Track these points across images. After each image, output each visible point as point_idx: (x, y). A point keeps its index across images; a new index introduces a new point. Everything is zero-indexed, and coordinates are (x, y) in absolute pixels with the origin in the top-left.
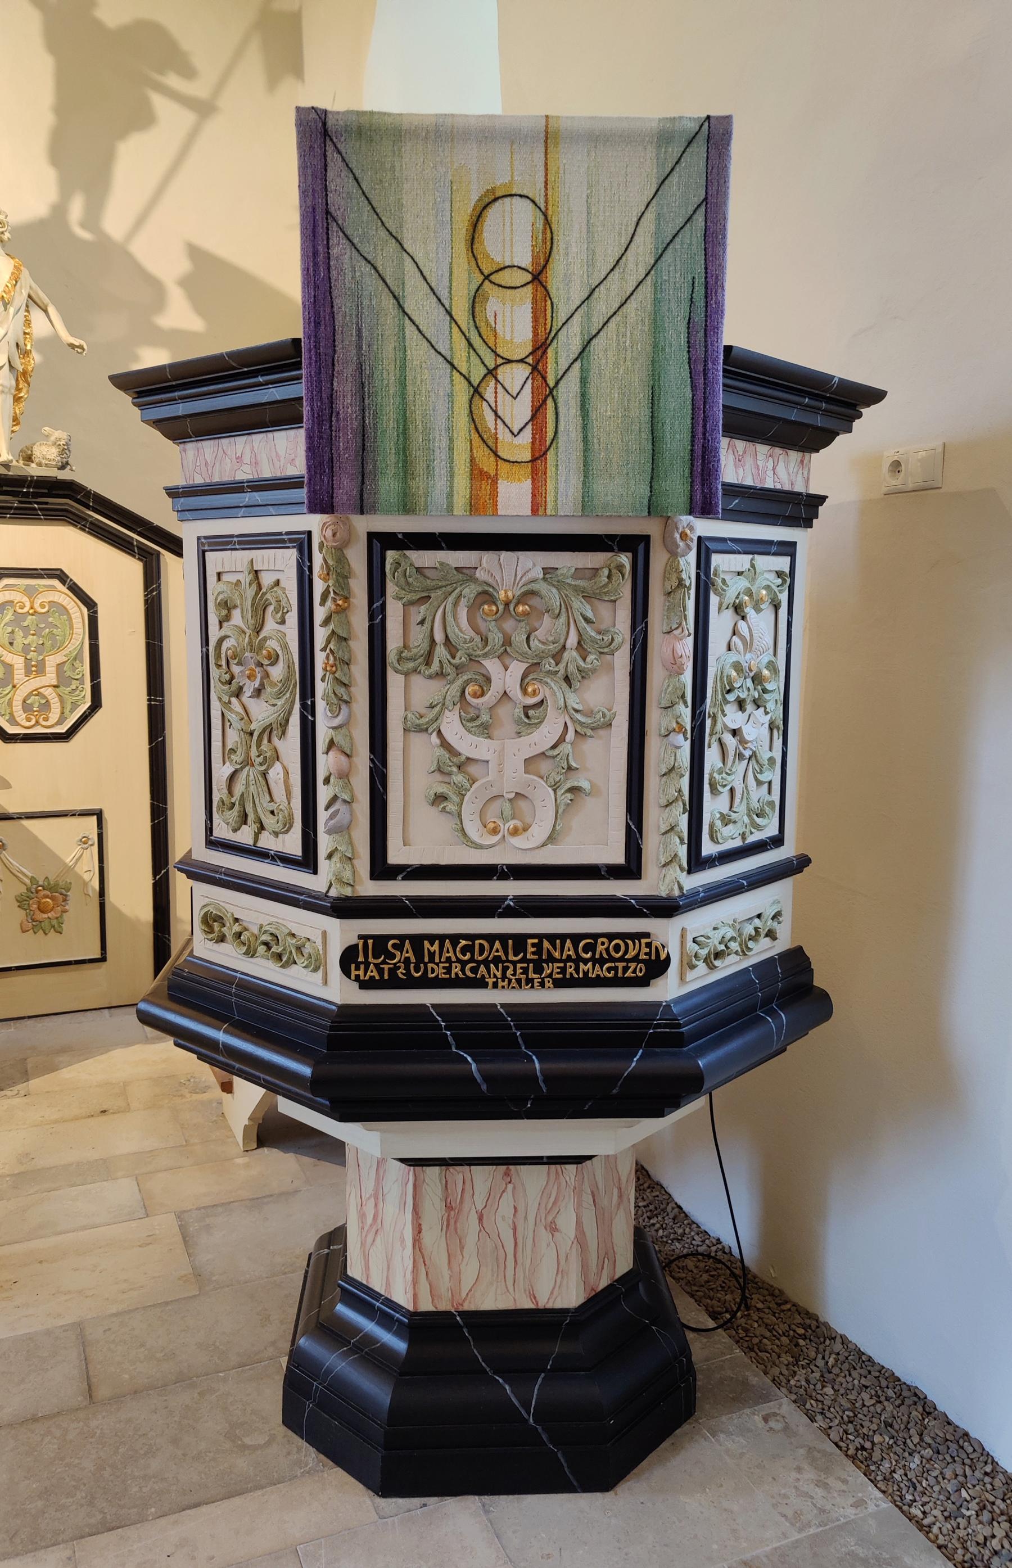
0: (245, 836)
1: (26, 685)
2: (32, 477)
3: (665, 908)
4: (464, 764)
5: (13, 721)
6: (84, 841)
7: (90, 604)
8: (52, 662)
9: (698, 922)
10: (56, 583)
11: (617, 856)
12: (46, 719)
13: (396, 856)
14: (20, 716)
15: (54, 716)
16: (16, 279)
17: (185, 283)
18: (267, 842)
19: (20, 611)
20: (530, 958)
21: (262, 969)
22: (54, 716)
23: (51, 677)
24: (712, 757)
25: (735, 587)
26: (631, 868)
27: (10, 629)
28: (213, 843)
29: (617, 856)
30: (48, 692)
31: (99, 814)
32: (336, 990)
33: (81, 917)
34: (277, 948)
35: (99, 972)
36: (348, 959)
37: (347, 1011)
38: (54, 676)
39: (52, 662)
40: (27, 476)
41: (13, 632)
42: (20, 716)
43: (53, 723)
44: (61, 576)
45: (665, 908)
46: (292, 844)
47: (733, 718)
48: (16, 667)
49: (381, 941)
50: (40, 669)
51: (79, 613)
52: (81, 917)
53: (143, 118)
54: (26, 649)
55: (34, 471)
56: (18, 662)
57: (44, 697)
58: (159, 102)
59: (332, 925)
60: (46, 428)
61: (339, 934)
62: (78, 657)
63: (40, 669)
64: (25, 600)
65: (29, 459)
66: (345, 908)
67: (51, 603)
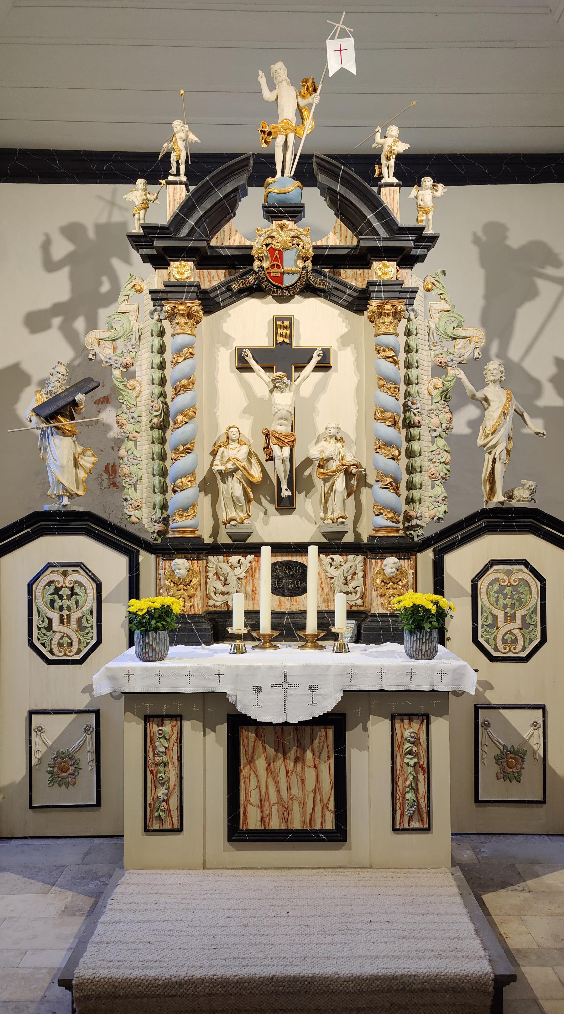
1: (504, 628)
2: (515, 508)
5: (496, 649)
6: (535, 724)
7: (542, 580)
8: (519, 614)
10: (523, 567)
12: (515, 648)
14: (500, 646)
15: (519, 647)
16: (509, 400)
17: (552, 380)
19: (502, 584)
22: (519, 647)
23: (518, 623)
27: (496, 595)
30: (517, 632)
31: (543, 708)
35: (539, 811)
38: (520, 622)
39: (519, 614)
40: (512, 508)
41: (498, 597)
42: (500, 646)
43: (518, 651)
44: (525, 563)
48: (499, 617)
50: (513, 618)
51: (535, 585)
53: (532, 293)
54: (505, 606)
55: (515, 504)
56: (500, 614)
57: (514, 635)
58: (541, 283)
60: (524, 480)
62: (534, 611)
63: (513, 618)
64: (506, 578)
65: (511, 497)
67: (520, 579)
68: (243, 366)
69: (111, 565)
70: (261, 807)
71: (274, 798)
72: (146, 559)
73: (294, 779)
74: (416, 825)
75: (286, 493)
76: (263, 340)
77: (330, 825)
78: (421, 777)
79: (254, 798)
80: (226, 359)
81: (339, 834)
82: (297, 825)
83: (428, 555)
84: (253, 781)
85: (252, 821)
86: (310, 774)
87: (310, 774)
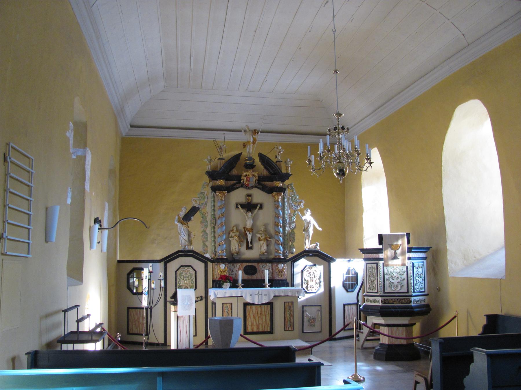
0: (371, 291)
3: (411, 296)
4: (392, 283)
6: (318, 311)
9: (415, 298)
11: (406, 291)
13: (386, 291)
18: (373, 291)
20: (398, 301)
21: (373, 304)
24: (415, 282)
25: (417, 266)
26: (408, 292)
28: (367, 292)
29: (406, 291)
32: (380, 304)
33: (317, 324)
34: (375, 301)
35: (320, 334)
36: (381, 301)
37: (381, 307)
45: (411, 296)
46: (376, 291)
47: (417, 278)
49: (384, 299)
52: (317, 324)
59: (380, 298)
61: (380, 299)
66: (381, 296)
68: (237, 207)
69: (199, 266)
70: (252, 326)
71: (255, 324)
72: (210, 264)
73: (260, 319)
74: (290, 329)
75: (250, 245)
76: (243, 200)
77: (269, 330)
78: (292, 318)
79: (250, 324)
80: (233, 206)
81: (271, 332)
82: (261, 330)
83: (290, 262)
84: (250, 320)
85: (249, 330)
86: (264, 318)
87: (264, 318)
